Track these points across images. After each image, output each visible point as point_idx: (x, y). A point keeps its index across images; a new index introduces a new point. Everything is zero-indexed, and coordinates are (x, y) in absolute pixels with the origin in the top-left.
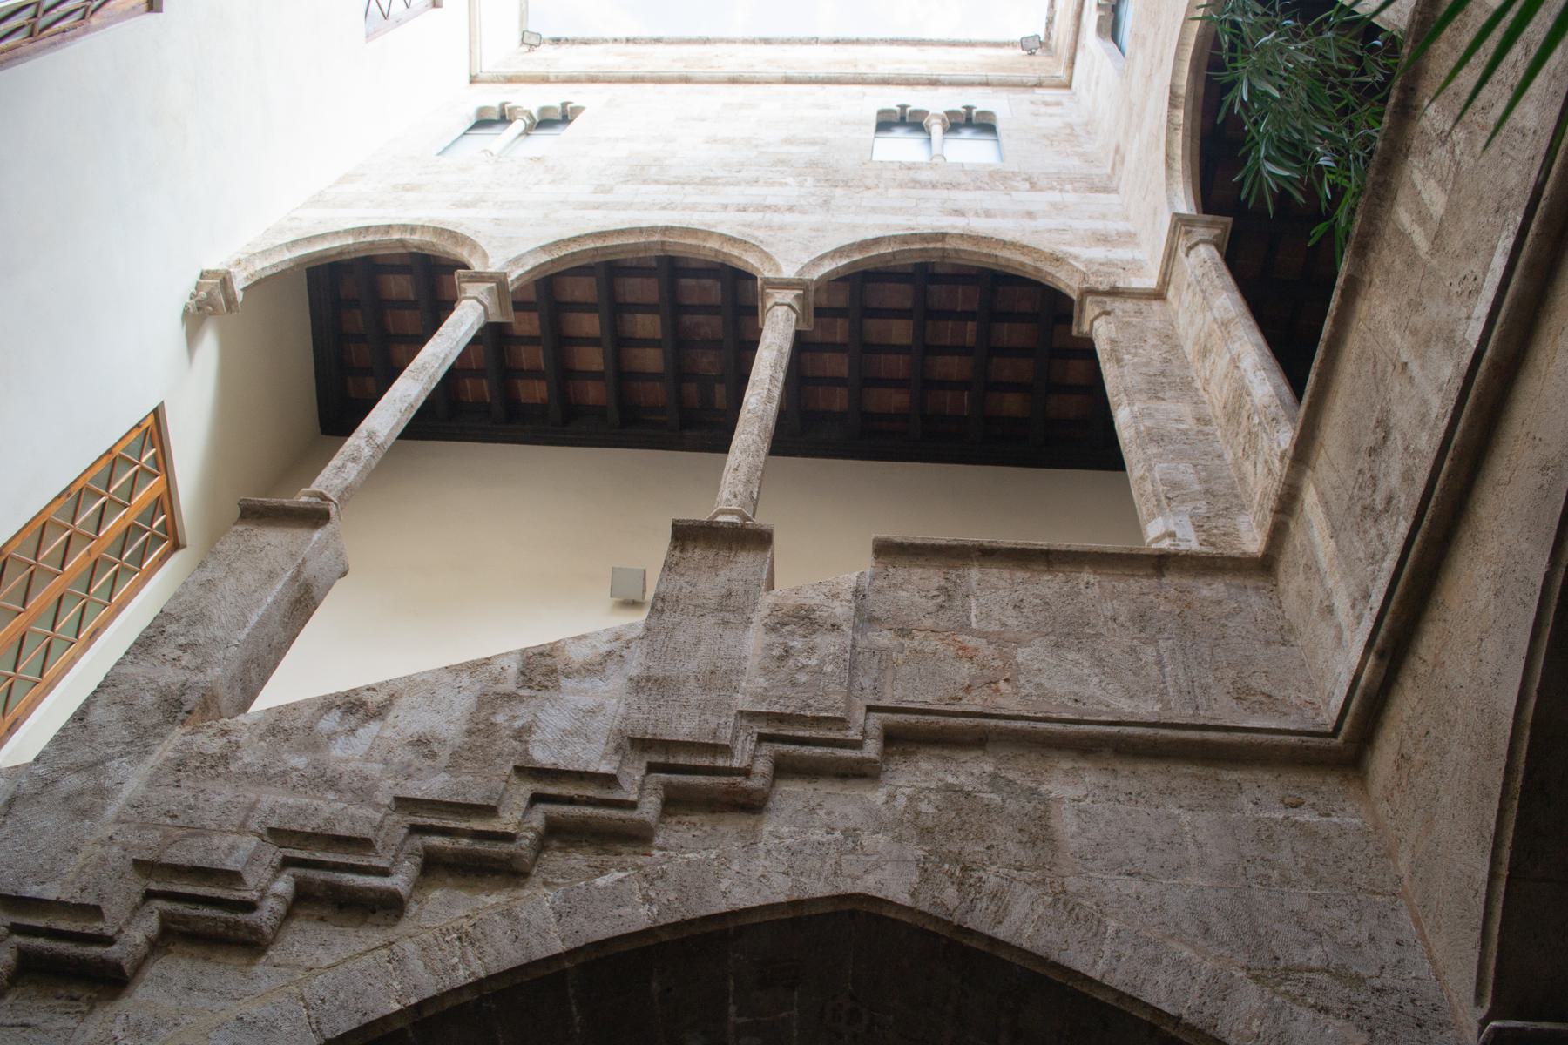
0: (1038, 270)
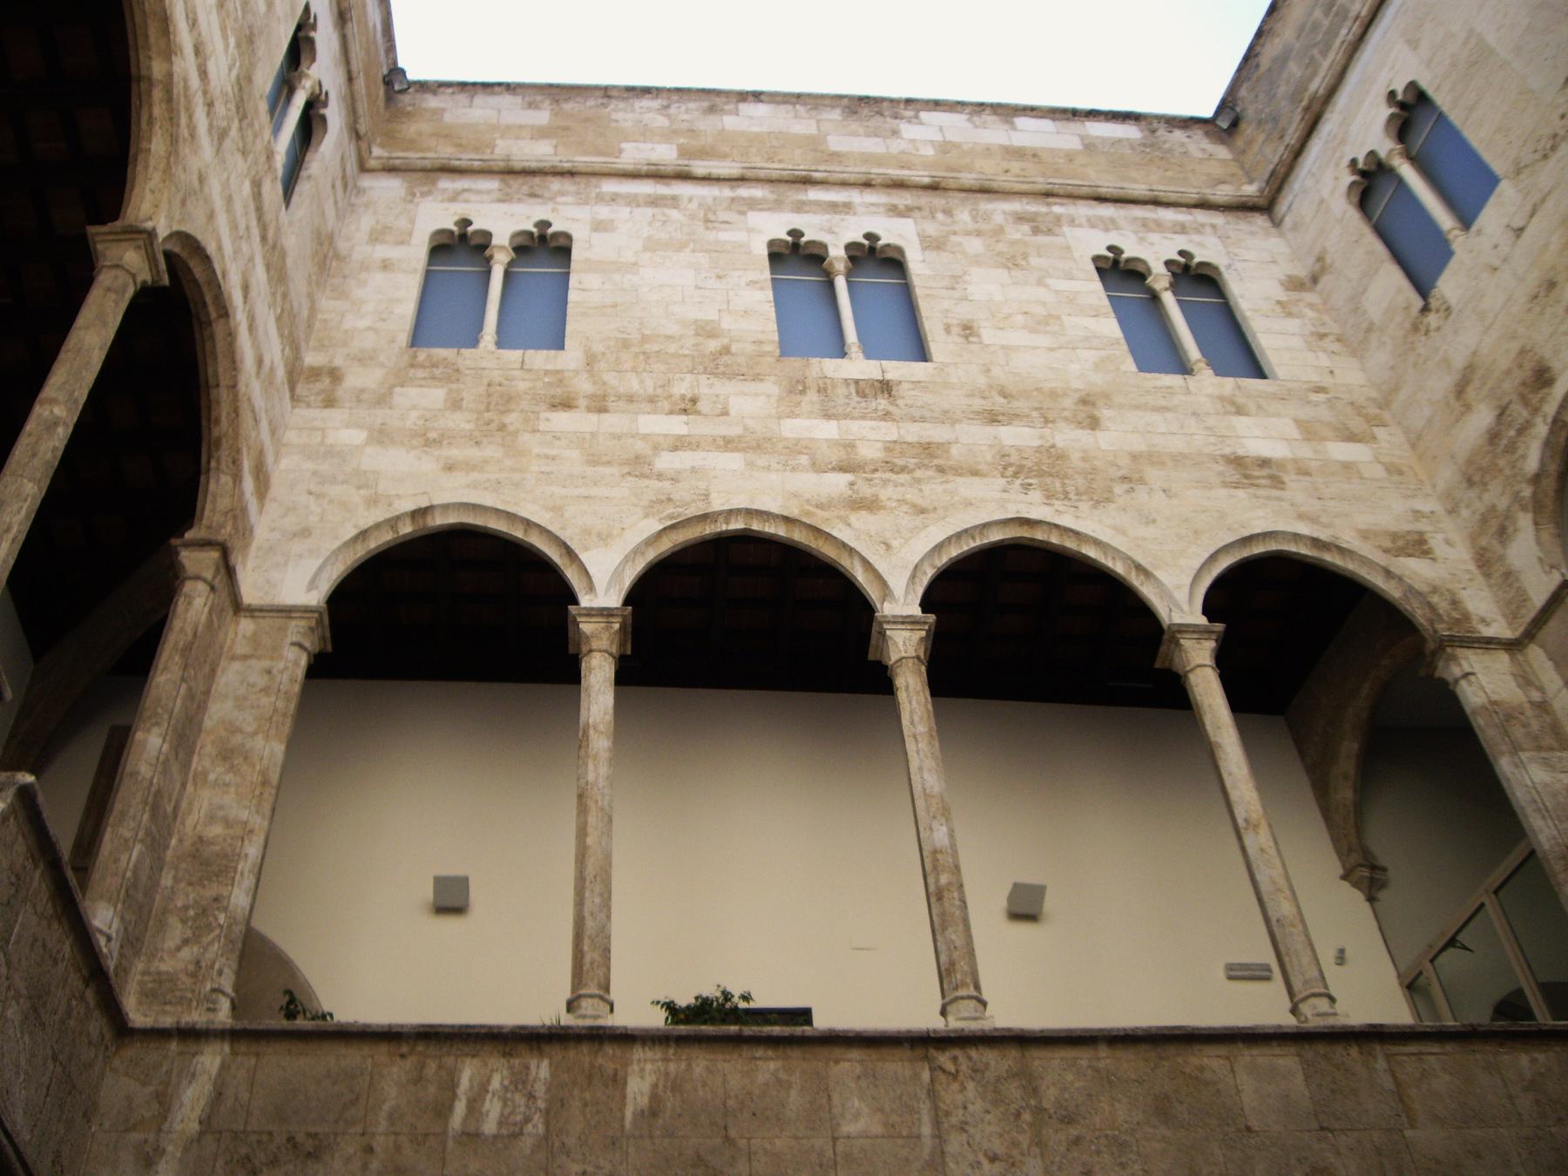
0: (218, 443)
